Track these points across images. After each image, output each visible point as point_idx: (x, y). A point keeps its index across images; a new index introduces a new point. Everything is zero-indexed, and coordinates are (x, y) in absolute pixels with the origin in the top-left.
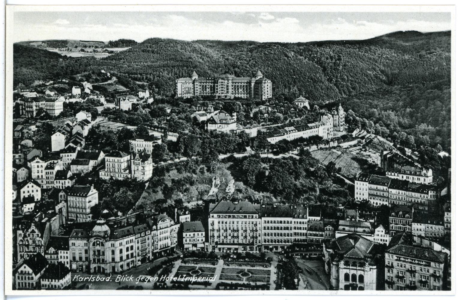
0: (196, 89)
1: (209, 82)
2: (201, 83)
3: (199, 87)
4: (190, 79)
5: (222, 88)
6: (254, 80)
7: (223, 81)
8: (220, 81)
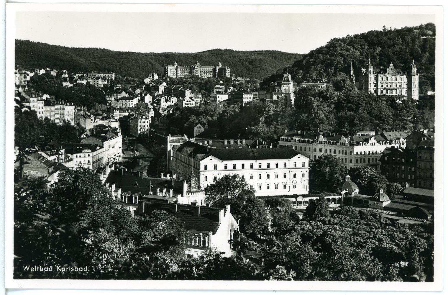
0: (178, 73)
1: (186, 69)
2: (180, 69)
3: (180, 72)
4: (173, 66)
5: (197, 72)
6: (217, 68)
7: (198, 68)
8: (196, 67)
